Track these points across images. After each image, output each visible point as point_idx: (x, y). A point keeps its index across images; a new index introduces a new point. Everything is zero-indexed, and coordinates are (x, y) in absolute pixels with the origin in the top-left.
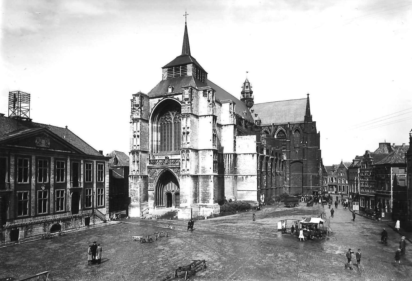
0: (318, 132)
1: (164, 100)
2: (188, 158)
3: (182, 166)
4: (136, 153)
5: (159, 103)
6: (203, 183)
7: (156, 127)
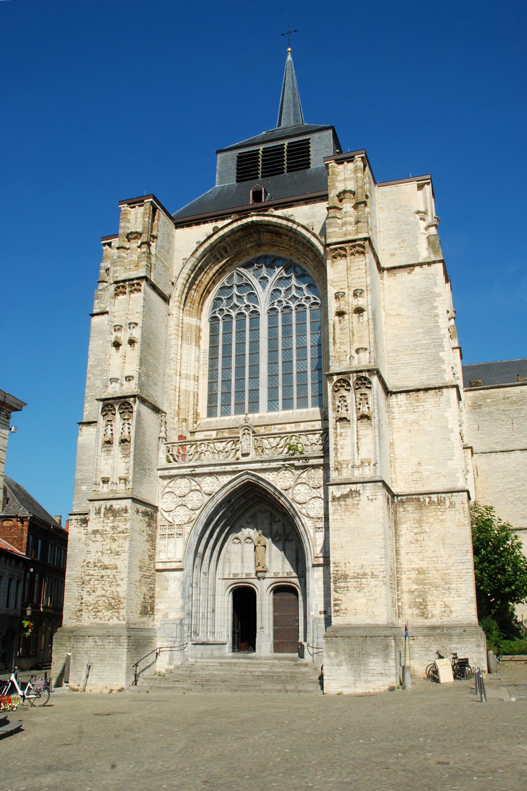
1: (235, 225)
2: (364, 410)
3: (336, 444)
4: (120, 408)
5: (215, 237)
6: (415, 531)
7: (194, 328)
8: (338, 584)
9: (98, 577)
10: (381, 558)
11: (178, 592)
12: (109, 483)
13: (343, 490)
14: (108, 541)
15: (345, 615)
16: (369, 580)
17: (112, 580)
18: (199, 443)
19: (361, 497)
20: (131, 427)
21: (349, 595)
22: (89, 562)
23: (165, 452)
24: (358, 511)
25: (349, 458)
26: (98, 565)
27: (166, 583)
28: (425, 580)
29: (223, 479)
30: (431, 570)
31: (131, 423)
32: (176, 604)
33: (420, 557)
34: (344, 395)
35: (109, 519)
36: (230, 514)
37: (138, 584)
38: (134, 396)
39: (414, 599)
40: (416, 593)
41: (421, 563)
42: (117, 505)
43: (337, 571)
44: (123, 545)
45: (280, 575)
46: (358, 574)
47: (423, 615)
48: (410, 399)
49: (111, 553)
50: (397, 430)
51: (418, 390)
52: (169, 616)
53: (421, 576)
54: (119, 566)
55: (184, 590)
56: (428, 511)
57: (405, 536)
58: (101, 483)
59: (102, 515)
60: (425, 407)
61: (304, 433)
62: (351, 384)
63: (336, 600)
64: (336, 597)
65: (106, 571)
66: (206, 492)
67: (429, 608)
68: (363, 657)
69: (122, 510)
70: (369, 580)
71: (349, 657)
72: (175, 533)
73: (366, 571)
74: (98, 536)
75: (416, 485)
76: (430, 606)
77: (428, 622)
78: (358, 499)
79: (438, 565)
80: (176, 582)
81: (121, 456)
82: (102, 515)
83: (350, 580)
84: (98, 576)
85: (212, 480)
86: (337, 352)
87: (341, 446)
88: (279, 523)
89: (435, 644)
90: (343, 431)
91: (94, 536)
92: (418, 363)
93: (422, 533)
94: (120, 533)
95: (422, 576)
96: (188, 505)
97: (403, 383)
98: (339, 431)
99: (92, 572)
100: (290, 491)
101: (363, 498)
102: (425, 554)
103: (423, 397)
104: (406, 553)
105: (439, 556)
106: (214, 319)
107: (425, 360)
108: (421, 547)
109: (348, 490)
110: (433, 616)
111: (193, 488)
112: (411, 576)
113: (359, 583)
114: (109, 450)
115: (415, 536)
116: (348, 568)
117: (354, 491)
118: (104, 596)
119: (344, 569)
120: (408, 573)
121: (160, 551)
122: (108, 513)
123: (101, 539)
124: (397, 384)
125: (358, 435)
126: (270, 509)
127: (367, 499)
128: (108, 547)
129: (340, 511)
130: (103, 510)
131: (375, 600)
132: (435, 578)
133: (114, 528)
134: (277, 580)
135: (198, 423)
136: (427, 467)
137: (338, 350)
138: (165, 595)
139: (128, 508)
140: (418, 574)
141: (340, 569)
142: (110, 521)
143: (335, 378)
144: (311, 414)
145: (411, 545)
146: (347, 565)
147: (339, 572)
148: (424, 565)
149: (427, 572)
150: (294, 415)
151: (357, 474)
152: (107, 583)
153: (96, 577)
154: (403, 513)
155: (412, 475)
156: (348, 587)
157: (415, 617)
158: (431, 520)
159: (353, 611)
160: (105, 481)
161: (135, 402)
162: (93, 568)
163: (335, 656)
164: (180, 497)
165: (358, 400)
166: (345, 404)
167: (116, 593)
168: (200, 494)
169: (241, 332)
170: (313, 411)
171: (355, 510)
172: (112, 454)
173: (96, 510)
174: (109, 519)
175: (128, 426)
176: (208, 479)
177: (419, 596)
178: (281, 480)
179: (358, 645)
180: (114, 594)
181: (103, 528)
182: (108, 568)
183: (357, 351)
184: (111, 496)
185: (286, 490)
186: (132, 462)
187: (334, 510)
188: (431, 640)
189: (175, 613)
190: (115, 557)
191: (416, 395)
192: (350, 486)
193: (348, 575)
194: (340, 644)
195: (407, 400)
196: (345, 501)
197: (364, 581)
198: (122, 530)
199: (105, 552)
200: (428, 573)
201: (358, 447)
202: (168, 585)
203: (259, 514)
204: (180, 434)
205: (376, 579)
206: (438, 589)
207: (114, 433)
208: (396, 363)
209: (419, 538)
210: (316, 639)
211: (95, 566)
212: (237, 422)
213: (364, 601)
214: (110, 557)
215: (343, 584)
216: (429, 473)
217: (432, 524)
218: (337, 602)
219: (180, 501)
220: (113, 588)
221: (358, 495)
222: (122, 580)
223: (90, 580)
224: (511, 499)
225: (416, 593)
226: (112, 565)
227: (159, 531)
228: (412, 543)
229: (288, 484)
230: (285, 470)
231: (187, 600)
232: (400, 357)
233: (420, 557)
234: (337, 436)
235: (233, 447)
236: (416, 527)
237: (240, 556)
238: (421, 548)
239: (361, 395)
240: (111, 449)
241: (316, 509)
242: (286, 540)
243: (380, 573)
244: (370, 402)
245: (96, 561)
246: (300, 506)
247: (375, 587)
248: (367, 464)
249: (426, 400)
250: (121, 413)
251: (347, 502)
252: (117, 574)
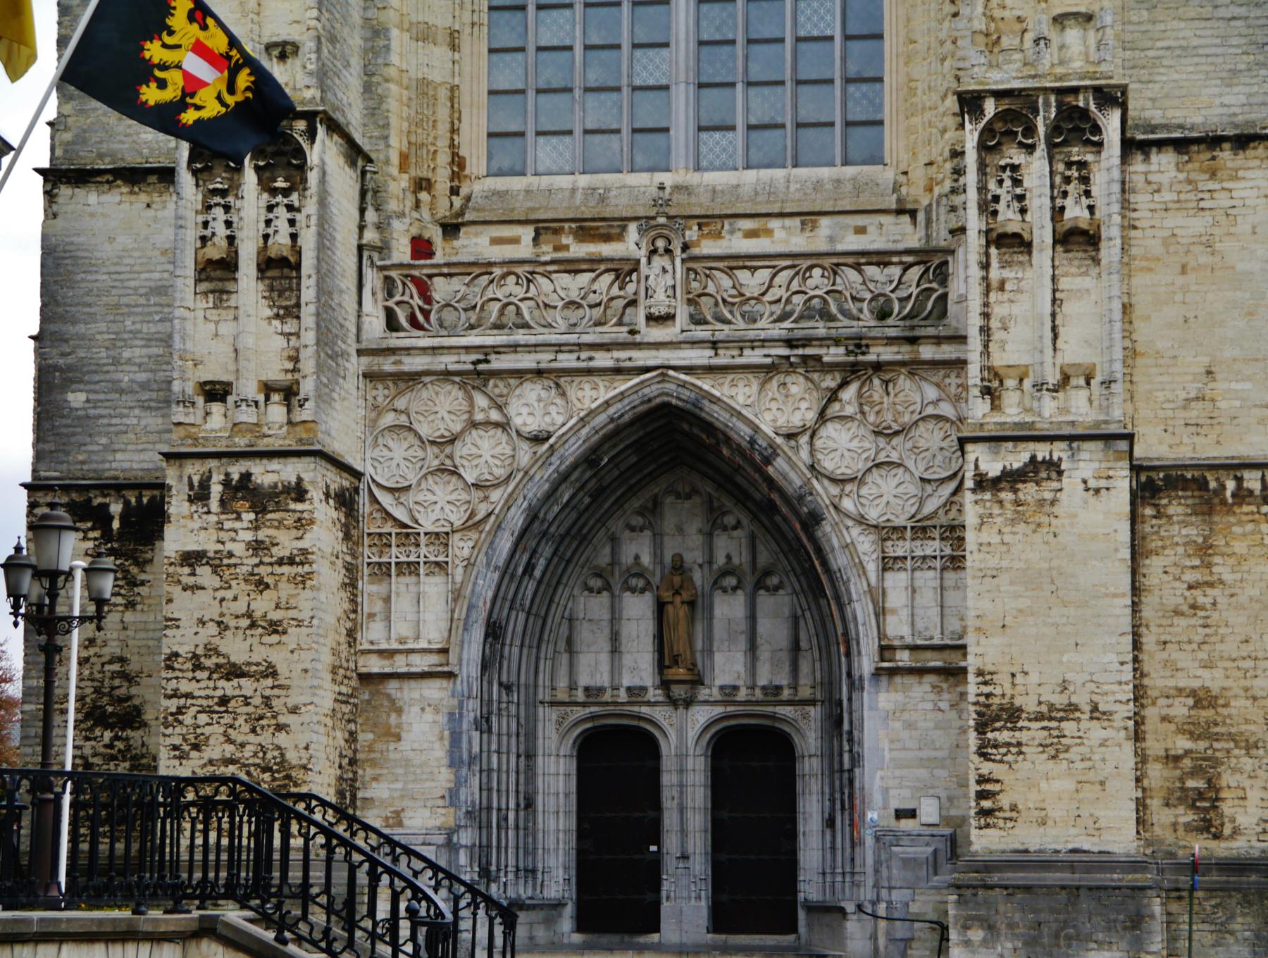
2: (1075, 212)
3: (986, 316)
6: (1190, 577)
8: (990, 735)
9: (211, 702)
10: (1122, 664)
11: (437, 745)
12: (231, 399)
13: (1011, 458)
14: (239, 587)
15: (1009, 824)
16: (1085, 724)
17: (260, 712)
18: (497, 271)
19: (1065, 480)
20: (299, 217)
21: (1023, 766)
22: (176, 655)
23: (380, 296)
24: (1054, 521)
25: (1024, 360)
26: (208, 663)
27: (393, 719)
28: (1216, 724)
29: (580, 394)
30: (1236, 696)
31: (296, 204)
32: (428, 784)
33: (1202, 655)
34: (1016, 161)
35: (239, 518)
36: (587, 500)
37: (329, 722)
38: (310, 116)
39: (1182, 780)
40: (1187, 763)
41: (1205, 674)
42: (266, 474)
43: (988, 696)
44: (293, 602)
45: (742, 695)
46: (1052, 707)
47: (1208, 826)
48: (1190, 166)
49: (253, 625)
50: (1144, 264)
51: (1213, 141)
52: (406, 822)
53: (1204, 713)
54: (282, 669)
55: (455, 739)
56: (1232, 519)
57: (1157, 592)
58: (200, 401)
59: (214, 505)
60: (1234, 194)
61: (850, 260)
62: (1041, 129)
63: (982, 780)
64: (985, 771)
65: (235, 682)
66: (525, 430)
67: (1226, 808)
68: (1069, 946)
69: (287, 490)
70: (1085, 724)
71: (1026, 944)
72: (422, 560)
73: (1074, 700)
74: (205, 575)
75: (1196, 439)
76: (1230, 803)
77: (1221, 849)
78: (1055, 485)
79: (1258, 683)
80: (429, 716)
81: (269, 313)
82: (214, 505)
83: (1026, 724)
84: (208, 697)
85: (544, 394)
86: (993, 19)
87: (1002, 320)
88: (736, 533)
89: (1244, 915)
90: (1007, 273)
91: (187, 570)
92: (1219, 51)
93: (1211, 585)
94: (280, 562)
95: (1207, 714)
96: (461, 471)
97: (1170, 114)
98: (995, 273)
99: (185, 687)
100: (804, 440)
101: (1071, 483)
102: (1219, 647)
103: (1229, 164)
104: (1158, 643)
105: (1260, 655)
107: (1243, 41)
108: (1205, 626)
109: (1025, 457)
110: (1236, 832)
111: (479, 417)
112: (1172, 712)
113: (1055, 733)
114: (223, 292)
115: (1187, 594)
116: (1020, 689)
117: (1044, 461)
118: (232, 761)
119: (1009, 692)
120: (1162, 702)
121: (371, 616)
122: (234, 498)
123: (216, 582)
124: (1147, 114)
125: (1054, 291)
126: (708, 488)
127: (1083, 486)
128: (241, 607)
129: (999, 520)
130: (216, 489)
131: (1102, 783)
132: (1247, 721)
133: (257, 547)
134: (730, 709)
135: (464, 191)
136: (1233, 385)
137: (998, 13)
138: (392, 756)
139: (306, 485)
140: (1195, 706)
141: (998, 691)
142: (245, 525)
143: (990, 107)
144: (849, 187)
145: (1176, 620)
146: (1019, 679)
147: (996, 701)
148: (1212, 680)
149: (1221, 702)
150: (793, 187)
151: (1049, 411)
152: (241, 720)
153: (200, 702)
154: (1154, 521)
155: (1185, 408)
156: (1019, 744)
157: (1181, 832)
158: (1239, 547)
159: (1037, 813)
160: (216, 392)
161: (311, 135)
162: (190, 675)
163: (985, 942)
164: (433, 443)
165: (1058, 179)
166: (1018, 191)
167: (276, 753)
168: (504, 438)
170: (854, 179)
171: (1045, 520)
172: (232, 303)
173: (191, 486)
174: (239, 518)
175: (289, 216)
176: (533, 392)
177: (1195, 772)
178: (774, 405)
179: (1053, 911)
180: (269, 756)
181: (220, 547)
182: (243, 675)
183: (1060, 20)
184: (241, 443)
185: (790, 436)
186: (309, 337)
187: (981, 517)
188: (1234, 901)
189: (427, 813)
190: (266, 639)
191: (1208, 155)
192: (1032, 446)
193: (1020, 710)
194: (1002, 908)
195: (1179, 170)
196: (1016, 491)
197: (1069, 727)
198: (288, 554)
199: (232, 623)
200: (1225, 706)
201: (1054, 329)
202: (399, 726)
203: (669, 500)
204: (414, 231)
205: (1106, 724)
206: (1254, 752)
207: (239, 235)
208: (1149, 44)
209: (1201, 600)
210: (884, 893)
211: (197, 667)
212: (603, 199)
213: (1069, 785)
214: (249, 640)
215: (1004, 736)
216: (1237, 403)
217: (1242, 559)
218: (989, 787)
219: (433, 459)
220: (265, 738)
221: (1054, 475)
222: (294, 710)
223: (180, 711)
225: (1187, 763)
226: (258, 664)
227: (368, 553)
228: (1177, 613)
229: (796, 420)
230: (787, 373)
231: (464, 771)
232: (1162, 27)
233: (1202, 655)
234: (987, 293)
235: (615, 291)
236: (1193, 567)
237: (607, 631)
238: (1207, 630)
239: (1069, 165)
240: (230, 286)
241: (884, 500)
242: (759, 585)
243: (1118, 707)
244: (1095, 190)
245: (200, 651)
246: (834, 490)
247: (1101, 745)
248: (1082, 382)
249: (1241, 173)
250: (258, 169)
251: (1021, 495)
252: (276, 692)
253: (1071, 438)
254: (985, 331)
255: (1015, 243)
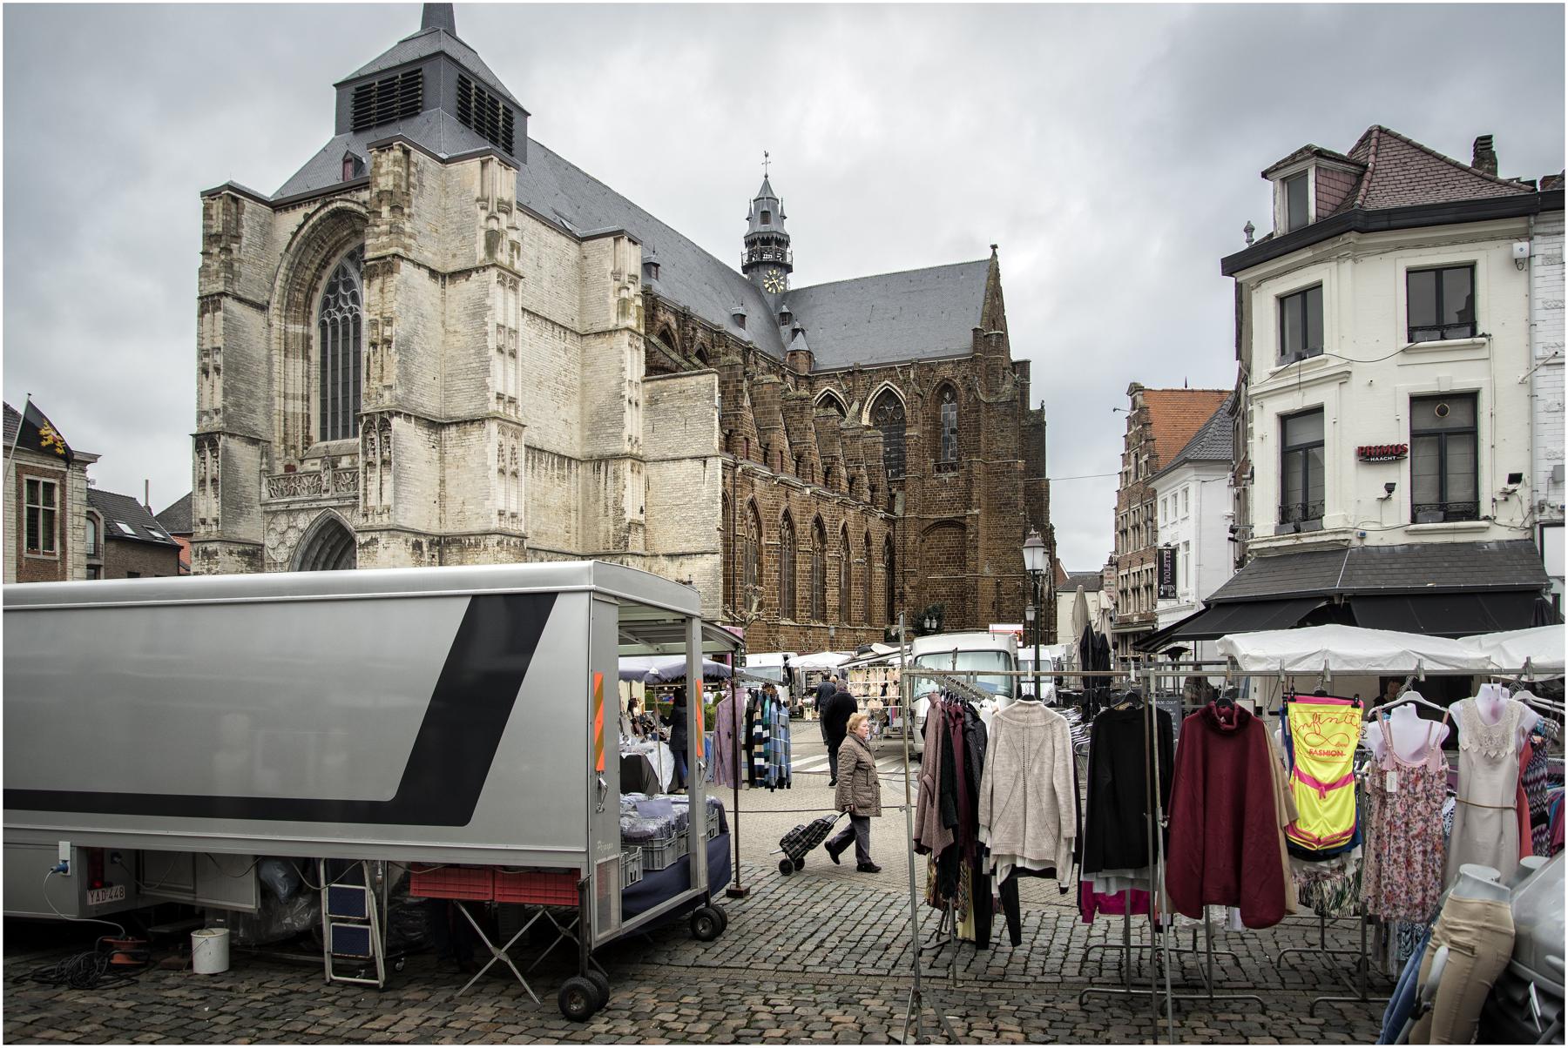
0: (1034, 406)
7: (300, 338)
106: (323, 325)
169: (346, 340)
201: (381, 494)
224: (677, 518)
253: (380, 531)
254: (365, 495)
255: (370, 464)
